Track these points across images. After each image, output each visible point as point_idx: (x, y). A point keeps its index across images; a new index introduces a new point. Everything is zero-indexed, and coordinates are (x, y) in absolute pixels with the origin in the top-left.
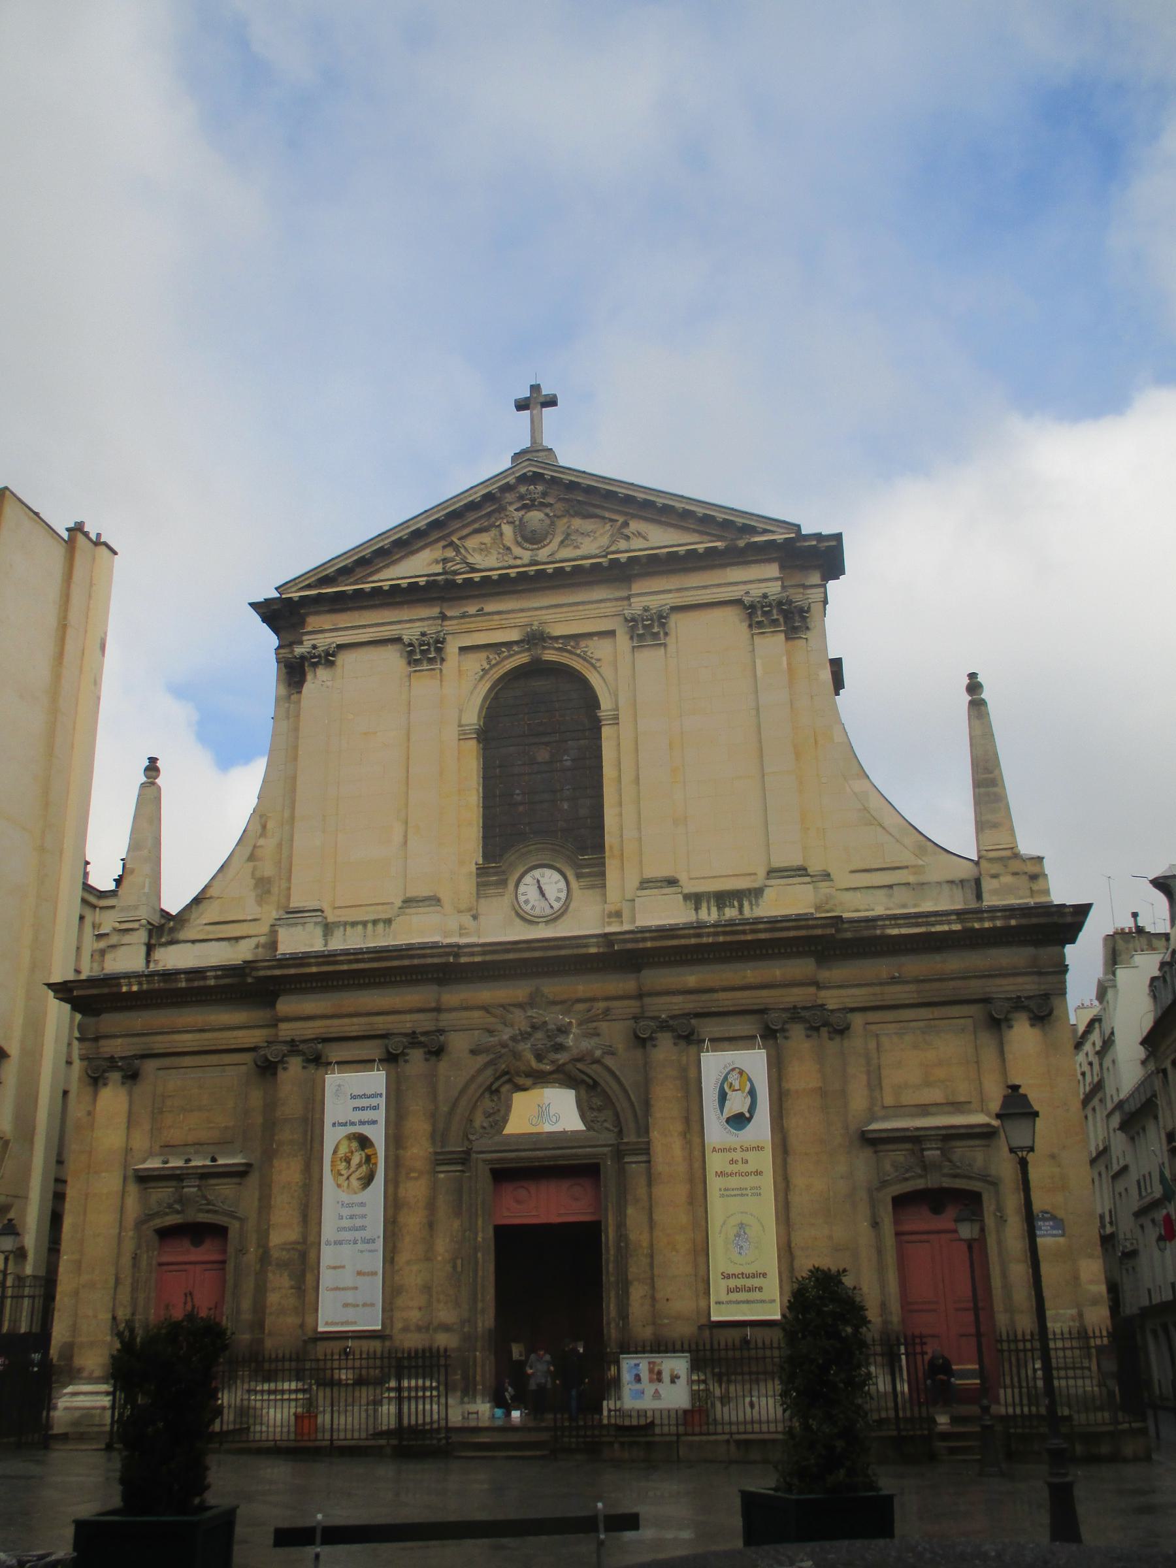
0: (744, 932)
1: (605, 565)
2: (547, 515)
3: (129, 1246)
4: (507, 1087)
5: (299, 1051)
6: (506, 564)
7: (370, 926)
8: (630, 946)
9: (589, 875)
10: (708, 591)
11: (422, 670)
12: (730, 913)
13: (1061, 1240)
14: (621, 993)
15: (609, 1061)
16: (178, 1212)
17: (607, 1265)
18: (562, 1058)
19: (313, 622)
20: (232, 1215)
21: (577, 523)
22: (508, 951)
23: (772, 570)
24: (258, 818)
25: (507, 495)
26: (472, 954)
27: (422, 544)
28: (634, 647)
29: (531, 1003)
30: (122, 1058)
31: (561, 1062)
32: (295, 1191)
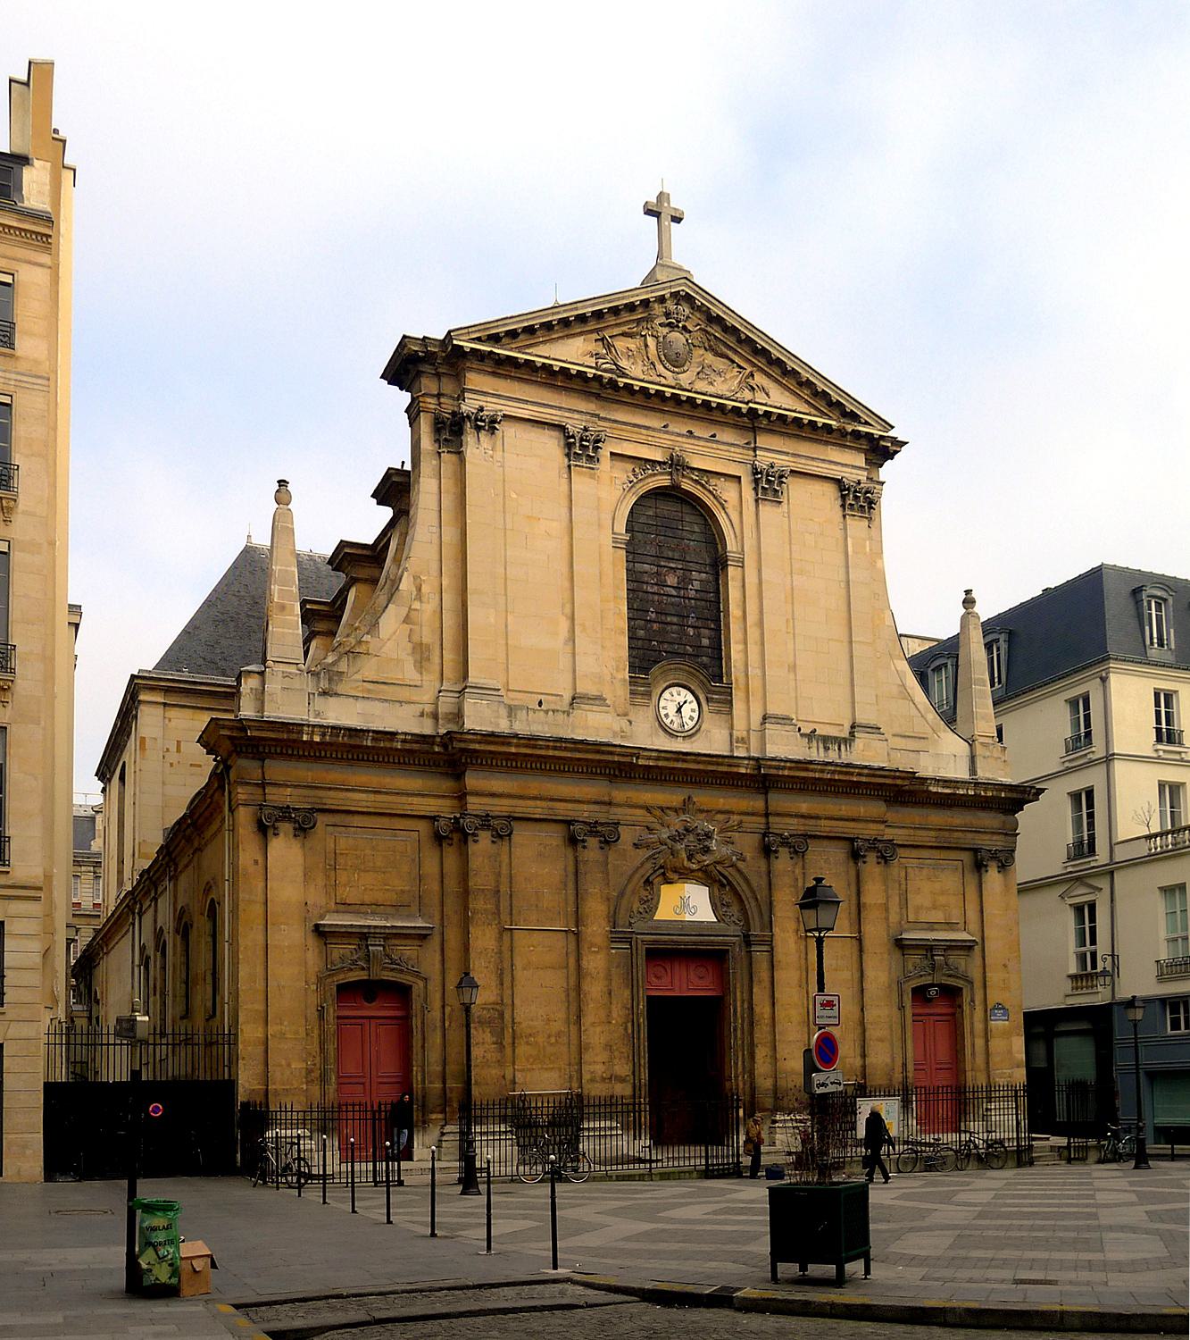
0: (852, 774)
1: (744, 411)
2: (687, 340)
3: (313, 1000)
4: (660, 879)
5: (490, 825)
6: (650, 379)
7: (551, 713)
8: (773, 772)
9: (718, 701)
10: (815, 464)
11: (582, 467)
12: (832, 756)
13: (1007, 1022)
14: (750, 810)
15: (740, 864)
16: (363, 969)
17: (735, 1030)
18: (707, 859)
19: (474, 380)
20: (417, 974)
21: (710, 358)
22: (677, 760)
23: (860, 460)
24: (412, 579)
25: (656, 305)
26: (649, 758)
27: (579, 330)
28: (757, 501)
29: (683, 808)
30: (294, 809)
31: (706, 863)
32: (492, 957)
